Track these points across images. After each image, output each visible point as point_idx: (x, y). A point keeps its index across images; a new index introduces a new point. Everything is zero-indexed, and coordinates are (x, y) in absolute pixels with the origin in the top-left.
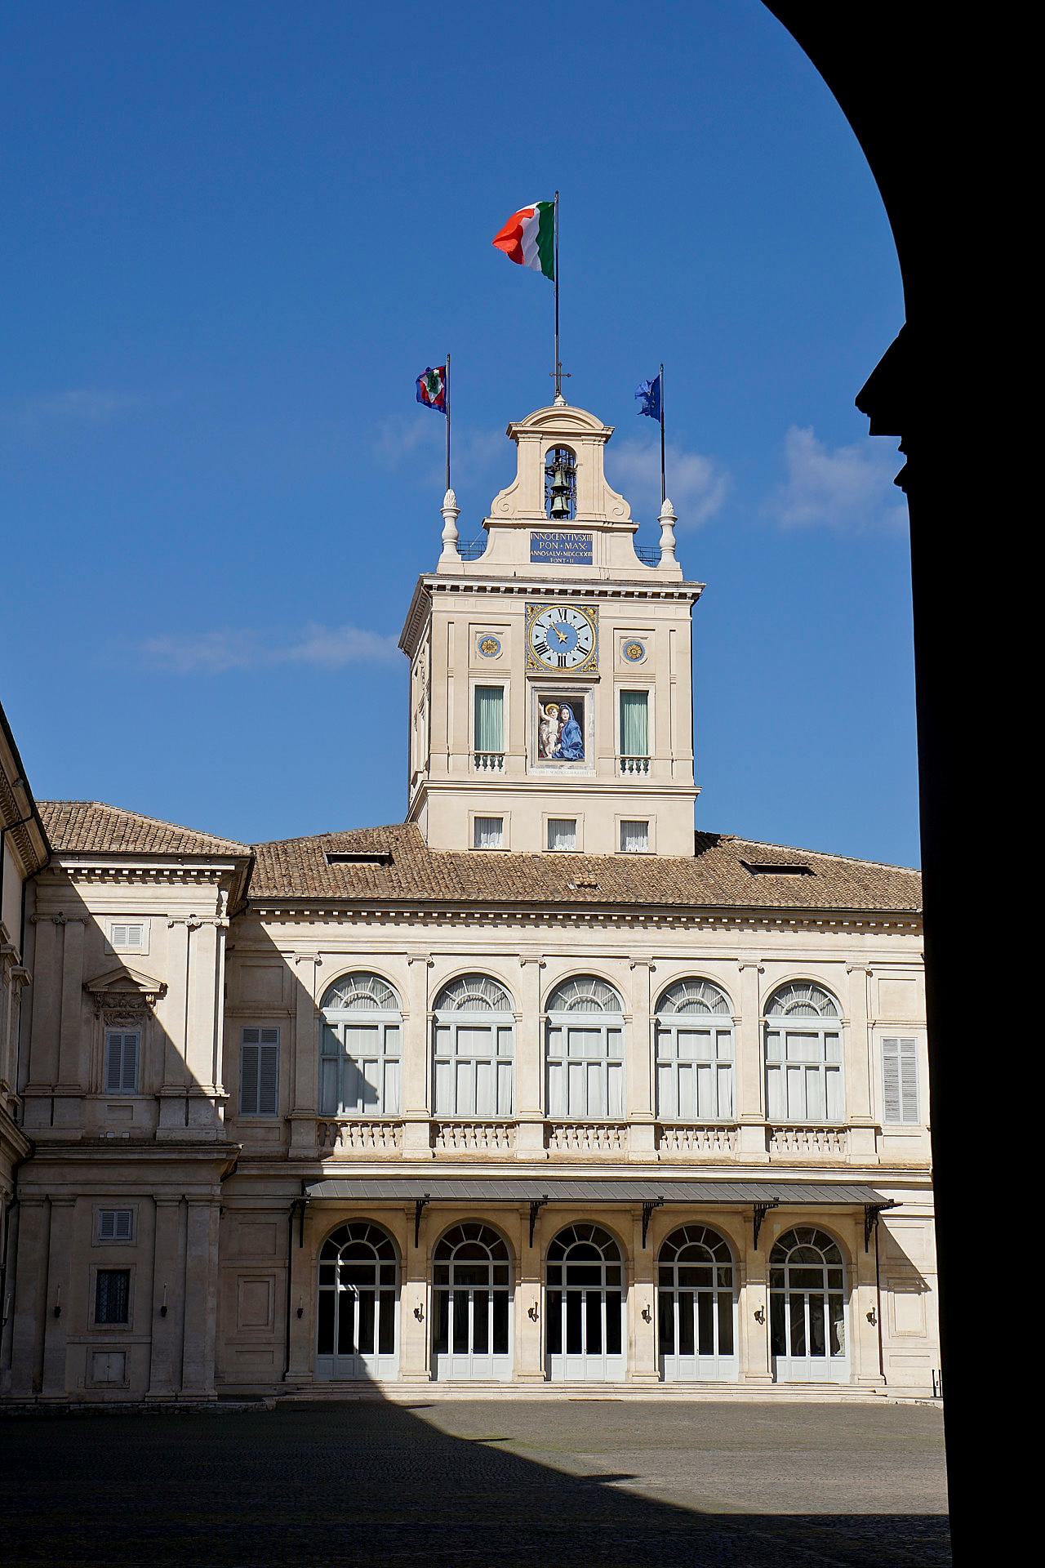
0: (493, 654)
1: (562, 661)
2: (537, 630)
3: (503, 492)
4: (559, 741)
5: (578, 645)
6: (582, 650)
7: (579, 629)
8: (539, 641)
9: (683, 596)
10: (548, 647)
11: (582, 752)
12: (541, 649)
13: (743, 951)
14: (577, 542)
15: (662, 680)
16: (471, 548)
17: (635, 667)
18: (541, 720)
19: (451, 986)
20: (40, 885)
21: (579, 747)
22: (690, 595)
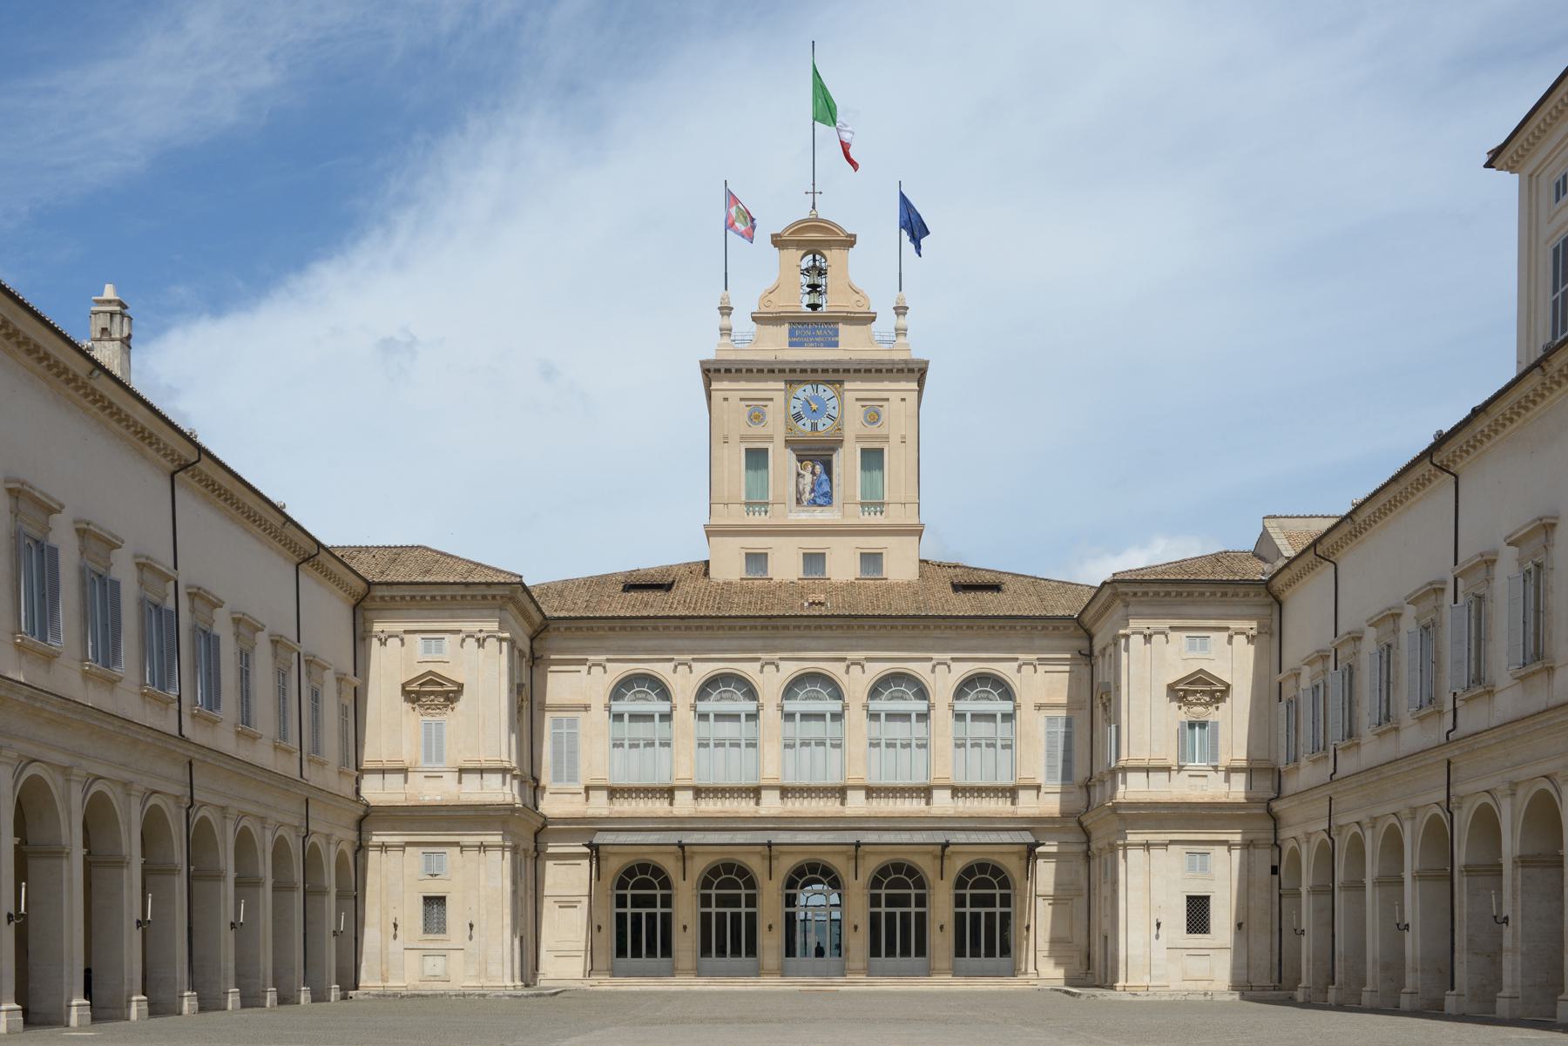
0: (760, 423)
1: (814, 427)
2: (794, 402)
4: (813, 490)
6: (830, 417)
9: (911, 371)
12: (798, 417)
15: (895, 439)
17: (874, 430)
18: (799, 475)
19: (639, 678)
20: (365, 609)
22: (916, 369)
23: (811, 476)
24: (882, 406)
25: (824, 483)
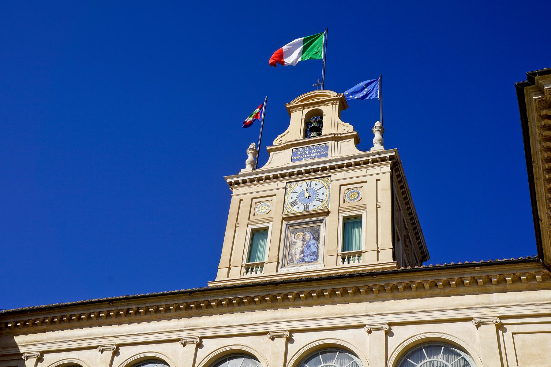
3: (280, 136)
4: (303, 252)
5: (317, 198)
7: (318, 190)
8: (293, 200)
9: (383, 160)
10: (298, 202)
11: (317, 257)
12: (294, 204)
13: (371, 318)
14: (320, 148)
16: (260, 161)
21: (315, 255)
23: (302, 242)
24: (361, 187)
25: (312, 246)
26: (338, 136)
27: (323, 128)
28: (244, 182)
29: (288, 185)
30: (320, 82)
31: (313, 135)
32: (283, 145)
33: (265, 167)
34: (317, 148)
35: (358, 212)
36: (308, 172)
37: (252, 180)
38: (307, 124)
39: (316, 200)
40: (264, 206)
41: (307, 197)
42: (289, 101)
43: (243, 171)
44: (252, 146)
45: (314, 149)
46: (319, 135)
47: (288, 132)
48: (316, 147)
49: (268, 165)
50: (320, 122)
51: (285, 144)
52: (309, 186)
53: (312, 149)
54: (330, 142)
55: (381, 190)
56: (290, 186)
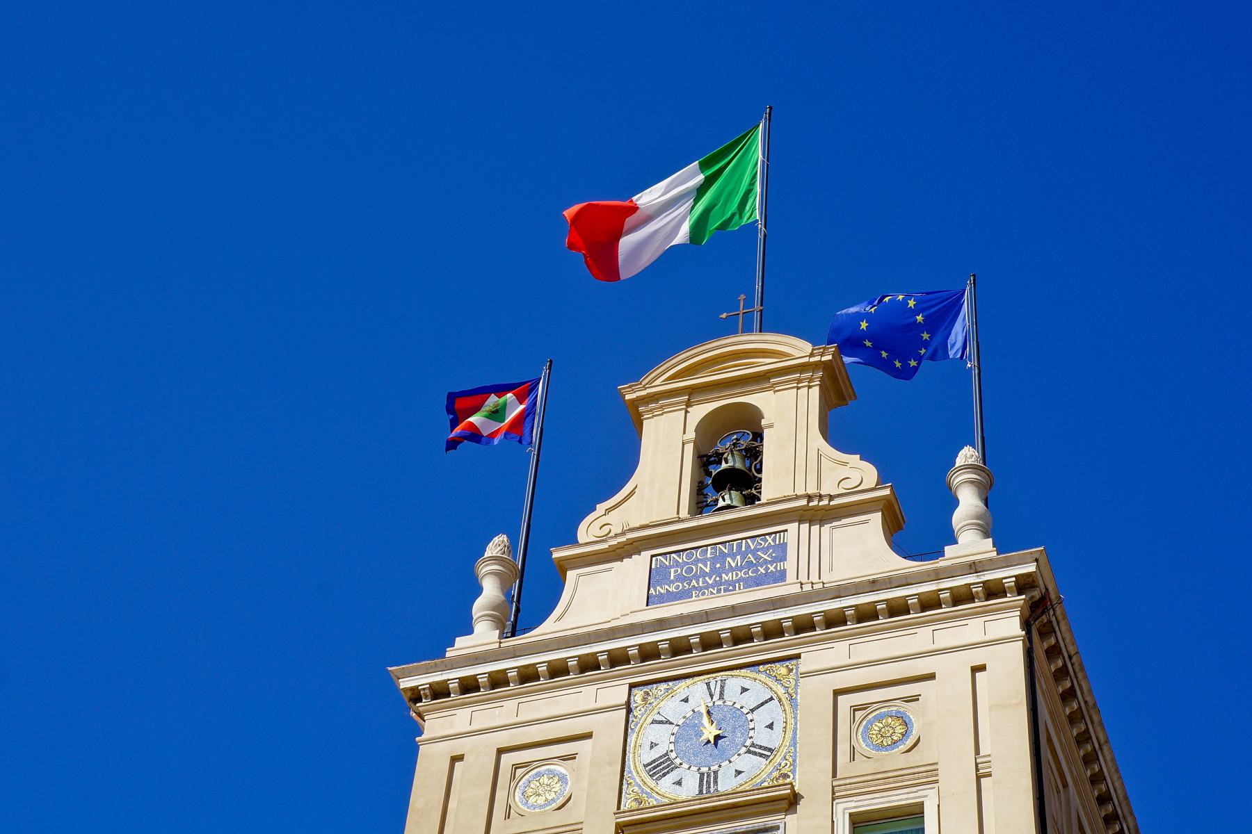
3: (601, 508)
5: (748, 743)
7: (752, 711)
8: (656, 753)
9: (994, 591)
10: (678, 761)
12: (660, 767)
14: (754, 552)
24: (915, 699)
26: (821, 504)
27: (764, 476)
28: (469, 686)
29: (638, 694)
30: (749, 303)
31: (728, 502)
32: (613, 542)
33: (548, 628)
34: (743, 549)
35: (905, 796)
36: (710, 642)
37: (498, 681)
38: (705, 460)
39: (744, 749)
40: (545, 780)
41: (709, 742)
42: (635, 375)
43: (463, 645)
44: (496, 546)
45: (733, 556)
46: (751, 500)
47: (632, 493)
48: (740, 546)
49: (559, 619)
50: (754, 454)
51: (623, 539)
52: (716, 697)
53: (723, 556)
54: (792, 527)
55: (990, 709)
56: (644, 699)
